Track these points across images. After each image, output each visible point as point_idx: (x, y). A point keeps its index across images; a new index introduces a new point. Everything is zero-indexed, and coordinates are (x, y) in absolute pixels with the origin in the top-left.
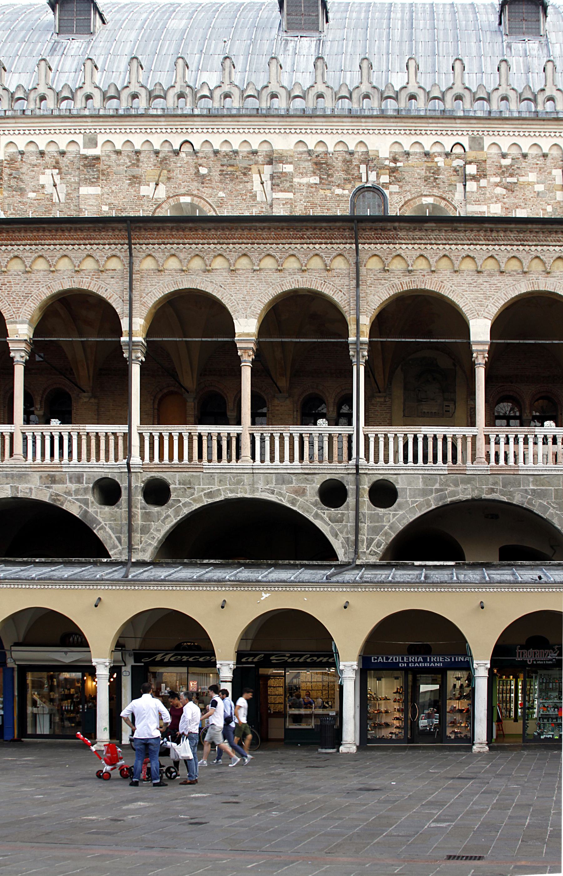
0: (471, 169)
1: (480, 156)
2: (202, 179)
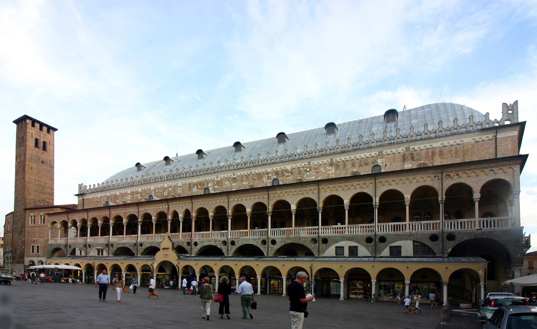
0: (308, 170)
1: (310, 166)
2: (254, 179)
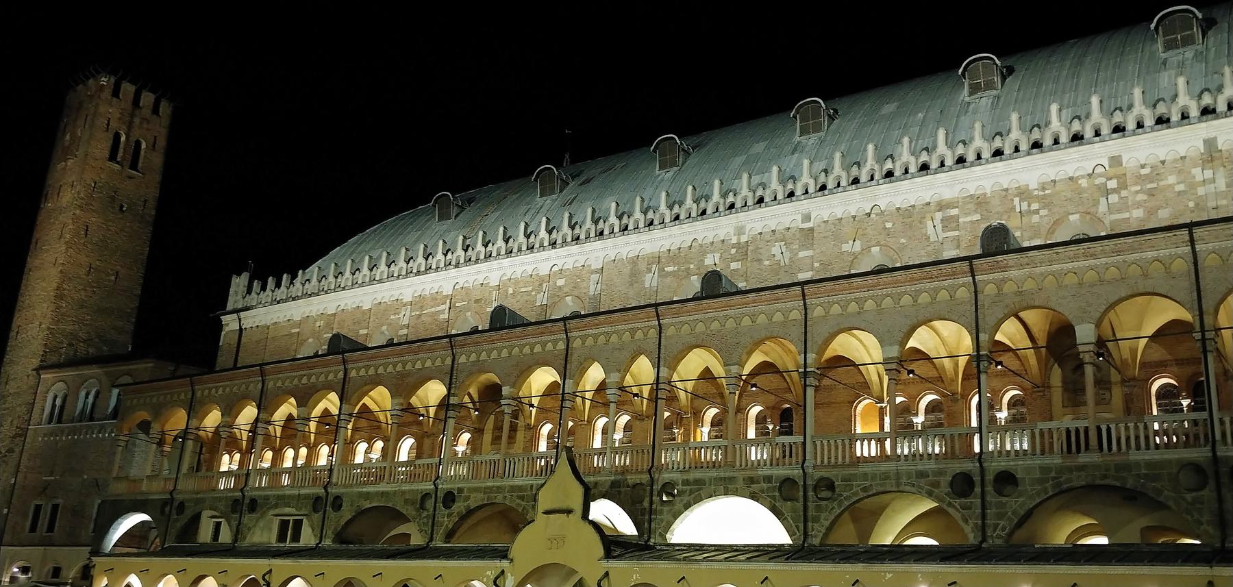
1: (1119, 171)
